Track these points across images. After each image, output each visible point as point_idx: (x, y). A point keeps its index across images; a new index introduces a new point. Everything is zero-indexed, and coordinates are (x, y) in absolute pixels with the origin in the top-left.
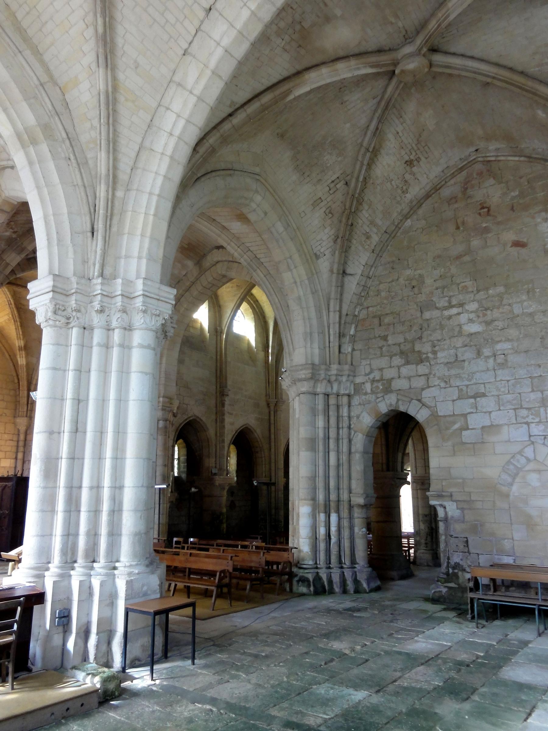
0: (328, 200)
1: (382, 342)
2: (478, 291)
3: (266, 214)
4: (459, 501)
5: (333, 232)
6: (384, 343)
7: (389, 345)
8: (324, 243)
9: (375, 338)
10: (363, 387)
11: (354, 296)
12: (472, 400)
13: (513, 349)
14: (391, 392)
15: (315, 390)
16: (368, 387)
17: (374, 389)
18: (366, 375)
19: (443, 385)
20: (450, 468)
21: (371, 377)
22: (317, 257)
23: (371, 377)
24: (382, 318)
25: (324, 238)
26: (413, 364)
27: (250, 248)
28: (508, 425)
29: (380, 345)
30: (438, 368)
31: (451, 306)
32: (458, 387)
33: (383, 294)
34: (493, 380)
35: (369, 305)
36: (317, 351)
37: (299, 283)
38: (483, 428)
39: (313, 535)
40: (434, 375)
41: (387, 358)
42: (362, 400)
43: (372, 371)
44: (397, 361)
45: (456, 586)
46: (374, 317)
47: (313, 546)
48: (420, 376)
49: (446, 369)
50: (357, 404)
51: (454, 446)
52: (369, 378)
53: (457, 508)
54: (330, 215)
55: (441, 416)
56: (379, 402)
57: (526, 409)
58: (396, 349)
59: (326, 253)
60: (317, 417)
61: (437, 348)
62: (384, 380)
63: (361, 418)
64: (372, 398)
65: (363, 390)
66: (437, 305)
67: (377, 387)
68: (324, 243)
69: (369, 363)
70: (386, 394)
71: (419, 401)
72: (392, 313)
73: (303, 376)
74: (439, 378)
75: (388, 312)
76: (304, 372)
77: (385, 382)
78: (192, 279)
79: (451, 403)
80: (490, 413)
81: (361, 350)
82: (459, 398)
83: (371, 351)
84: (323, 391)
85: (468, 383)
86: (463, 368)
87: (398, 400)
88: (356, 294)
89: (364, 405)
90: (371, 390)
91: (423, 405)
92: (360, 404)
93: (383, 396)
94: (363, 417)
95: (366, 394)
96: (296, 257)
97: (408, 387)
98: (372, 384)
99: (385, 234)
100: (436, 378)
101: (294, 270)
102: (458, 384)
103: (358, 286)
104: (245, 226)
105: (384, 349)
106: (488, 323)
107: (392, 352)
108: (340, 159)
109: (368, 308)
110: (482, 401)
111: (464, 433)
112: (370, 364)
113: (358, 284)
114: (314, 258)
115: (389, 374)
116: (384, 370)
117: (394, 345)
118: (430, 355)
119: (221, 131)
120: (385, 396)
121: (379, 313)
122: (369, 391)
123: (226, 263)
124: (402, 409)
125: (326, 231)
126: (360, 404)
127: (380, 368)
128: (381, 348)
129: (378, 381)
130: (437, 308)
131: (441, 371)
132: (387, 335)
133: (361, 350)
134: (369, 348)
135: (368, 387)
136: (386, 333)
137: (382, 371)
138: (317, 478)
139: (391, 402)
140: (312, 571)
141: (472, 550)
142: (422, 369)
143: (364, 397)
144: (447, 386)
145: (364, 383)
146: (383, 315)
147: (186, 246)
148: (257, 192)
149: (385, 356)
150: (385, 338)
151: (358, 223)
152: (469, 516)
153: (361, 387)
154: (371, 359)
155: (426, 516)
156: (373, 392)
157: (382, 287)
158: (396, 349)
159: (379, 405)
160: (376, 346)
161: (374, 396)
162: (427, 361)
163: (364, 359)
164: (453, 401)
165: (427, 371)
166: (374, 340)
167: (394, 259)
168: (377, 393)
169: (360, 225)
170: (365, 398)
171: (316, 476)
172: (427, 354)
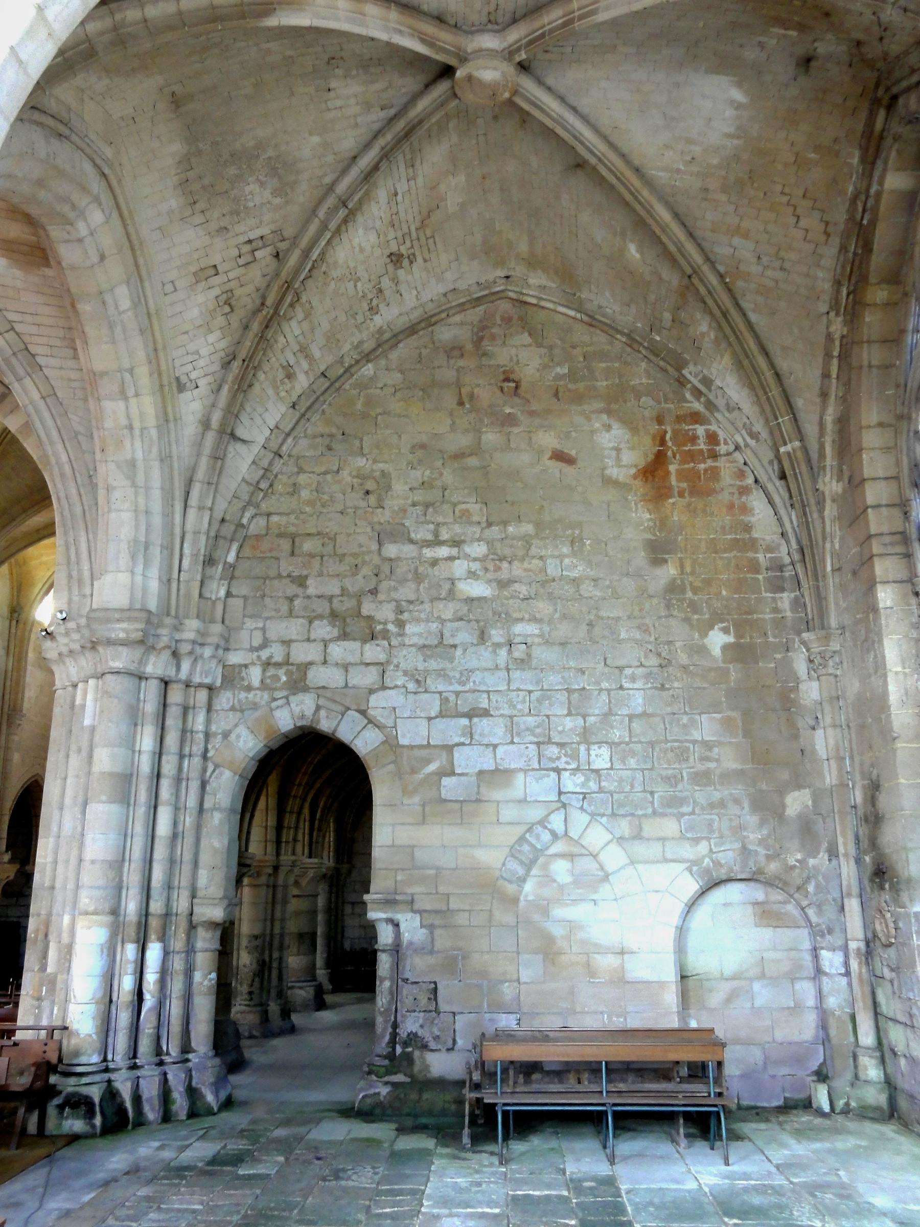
0: (231, 275)
1: (292, 589)
2: (490, 524)
3: (102, 258)
4: (425, 911)
5: (223, 344)
6: (300, 591)
7: (309, 597)
8: (202, 363)
9: (279, 576)
10: (243, 674)
11: (244, 485)
12: (465, 721)
13: (541, 636)
14: (306, 689)
15: (142, 669)
16: (255, 675)
17: (268, 681)
18: (253, 649)
19: (411, 686)
20: (413, 847)
21: (264, 654)
22: (181, 388)
23: (264, 654)
24: (297, 540)
25: (204, 352)
26: (355, 640)
27: (15, 325)
28: (526, 771)
30: (404, 652)
31: (437, 542)
32: (440, 693)
33: (305, 494)
34: (503, 687)
35: (272, 510)
36: (154, 585)
37: (137, 432)
38: (481, 773)
39: (105, 994)
40: (397, 666)
41: (301, 620)
42: (239, 701)
43: (265, 644)
44: (323, 629)
45: (408, 1080)
46: (280, 535)
47: (103, 1020)
48: (368, 664)
49: (421, 658)
50: (227, 707)
51: (424, 806)
52: (259, 657)
53: (422, 926)
54: (227, 309)
55: (403, 746)
56: (278, 707)
57: (557, 744)
58: (322, 607)
59: (201, 383)
60: (139, 728)
61: (406, 616)
62: (292, 664)
63: (233, 736)
64: (263, 697)
65: (243, 679)
66: (413, 535)
67: (276, 678)
68: (202, 363)
69: (260, 625)
70: (294, 694)
71: (363, 713)
72: (319, 534)
73: (122, 635)
74: (405, 673)
75: (314, 531)
76: (124, 625)
77: (294, 668)
79: (425, 723)
80: (495, 746)
81: (245, 598)
82: (441, 715)
83: (267, 600)
84: (159, 672)
85: (459, 688)
86: (451, 660)
87: (318, 708)
88: (247, 483)
89: (242, 711)
91: (370, 722)
92: (233, 709)
93: (287, 697)
94: (238, 736)
95: (249, 688)
96: (143, 372)
97: (341, 683)
98: (264, 671)
99: (322, 379)
100: (400, 673)
101: (133, 402)
102: (441, 688)
103: (253, 467)
104: (17, 273)
105: (297, 602)
106: (503, 584)
107: (314, 611)
108: (278, 201)
109: (269, 515)
110: (482, 724)
111: (446, 781)
112: (264, 630)
113: (254, 462)
114: (174, 384)
115: (302, 653)
116: (293, 645)
117: (319, 597)
118: (391, 627)
119: (118, 17)
120: (292, 698)
121: (292, 529)
122: (256, 682)
124: (325, 725)
125: (212, 338)
126: (233, 709)
127: (287, 638)
128: (291, 600)
129: (278, 665)
130: (411, 541)
131: (408, 659)
132: (306, 577)
133: (245, 598)
134: (263, 596)
135: (255, 675)
136: (305, 573)
137: (289, 646)
138: (127, 864)
139: (302, 711)
140: (97, 1078)
141: (443, 1007)
142: (374, 652)
143: (243, 695)
144: (420, 690)
145: (246, 666)
146: (299, 535)
148: (97, 200)
149: (297, 617)
150: (301, 581)
151: (276, 341)
152: (443, 941)
153: (239, 673)
154: (267, 618)
155: (256, 937)
156: (264, 686)
157: (302, 479)
158: (322, 607)
159: (277, 714)
160: (280, 594)
161: (266, 696)
162: (384, 638)
163: (251, 617)
164: (430, 719)
165: (382, 657)
167: (334, 430)
168: (276, 689)
169: (280, 346)
171: (123, 860)
172: (385, 623)
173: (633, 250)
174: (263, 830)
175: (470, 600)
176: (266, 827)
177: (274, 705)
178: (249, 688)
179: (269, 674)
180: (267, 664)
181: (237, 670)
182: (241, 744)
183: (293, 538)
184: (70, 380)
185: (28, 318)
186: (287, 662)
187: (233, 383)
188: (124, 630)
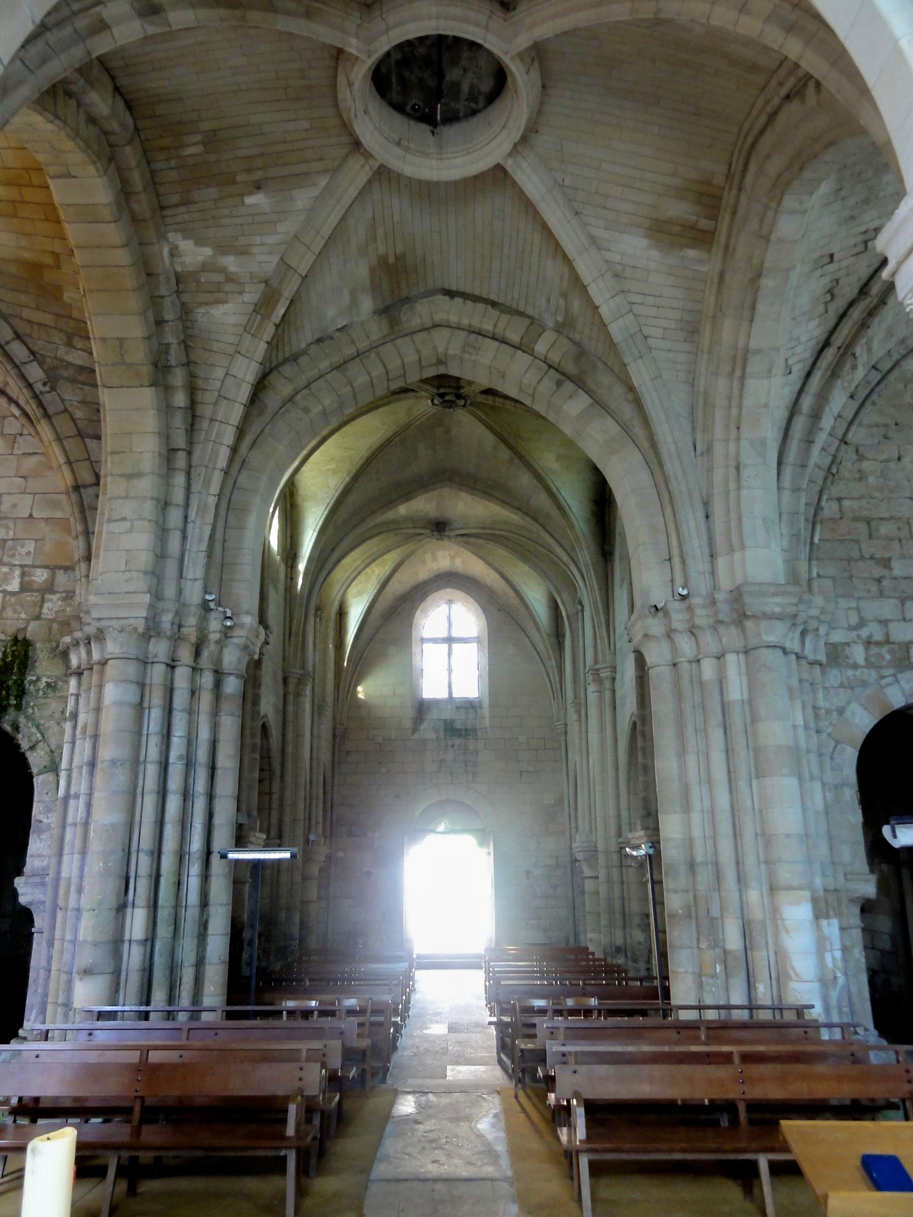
1: (878, 572)
5: (817, 332)
6: (886, 572)
7: (895, 578)
9: (862, 558)
10: (847, 652)
11: (817, 470)
16: (858, 653)
17: (873, 659)
18: (851, 628)
21: (864, 633)
23: (864, 633)
24: (873, 523)
25: (804, 339)
27: (634, 307)
29: (877, 576)
33: (871, 479)
35: (842, 495)
41: (893, 601)
42: (848, 678)
43: (862, 624)
46: (855, 519)
52: (859, 636)
54: (828, 297)
56: (887, 685)
62: (893, 643)
63: (848, 714)
65: (847, 657)
67: (881, 657)
69: (854, 605)
70: (902, 672)
72: (892, 518)
73: (777, 609)
75: (887, 515)
76: (778, 600)
77: (896, 646)
78: (363, 345)
81: (833, 578)
83: (856, 581)
88: (819, 467)
89: (852, 688)
90: (866, 660)
92: (842, 686)
93: (894, 675)
94: (853, 713)
95: (855, 666)
98: (867, 649)
99: (874, 372)
103: (823, 452)
104: (655, 254)
105: (885, 583)
107: (904, 592)
109: (839, 500)
112: (858, 609)
113: (823, 449)
116: (891, 625)
117: (906, 578)
120: (900, 676)
121: (865, 513)
122: (861, 660)
123: (463, 334)
126: (842, 686)
127: (883, 618)
128: (879, 581)
129: (878, 643)
132: (889, 559)
133: (833, 578)
134: (851, 577)
135: (858, 653)
136: (887, 555)
137: (886, 626)
143: (850, 673)
145: (848, 644)
146: (873, 519)
147: (391, 260)
149: (888, 598)
150: (886, 563)
153: (843, 650)
154: (859, 598)
156: (869, 664)
157: (865, 465)
159: (889, 691)
160: (867, 575)
161: (874, 674)
163: (843, 596)
166: (861, 563)
167: (888, 421)
168: (881, 667)
170: (854, 675)
177: (883, 682)
178: (855, 666)
179: (871, 652)
180: (868, 643)
181: (840, 649)
182: (857, 721)
183: (868, 521)
184: (675, 362)
185: (650, 300)
186: (888, 642)
187: (826, 370)
188: (778, 604)
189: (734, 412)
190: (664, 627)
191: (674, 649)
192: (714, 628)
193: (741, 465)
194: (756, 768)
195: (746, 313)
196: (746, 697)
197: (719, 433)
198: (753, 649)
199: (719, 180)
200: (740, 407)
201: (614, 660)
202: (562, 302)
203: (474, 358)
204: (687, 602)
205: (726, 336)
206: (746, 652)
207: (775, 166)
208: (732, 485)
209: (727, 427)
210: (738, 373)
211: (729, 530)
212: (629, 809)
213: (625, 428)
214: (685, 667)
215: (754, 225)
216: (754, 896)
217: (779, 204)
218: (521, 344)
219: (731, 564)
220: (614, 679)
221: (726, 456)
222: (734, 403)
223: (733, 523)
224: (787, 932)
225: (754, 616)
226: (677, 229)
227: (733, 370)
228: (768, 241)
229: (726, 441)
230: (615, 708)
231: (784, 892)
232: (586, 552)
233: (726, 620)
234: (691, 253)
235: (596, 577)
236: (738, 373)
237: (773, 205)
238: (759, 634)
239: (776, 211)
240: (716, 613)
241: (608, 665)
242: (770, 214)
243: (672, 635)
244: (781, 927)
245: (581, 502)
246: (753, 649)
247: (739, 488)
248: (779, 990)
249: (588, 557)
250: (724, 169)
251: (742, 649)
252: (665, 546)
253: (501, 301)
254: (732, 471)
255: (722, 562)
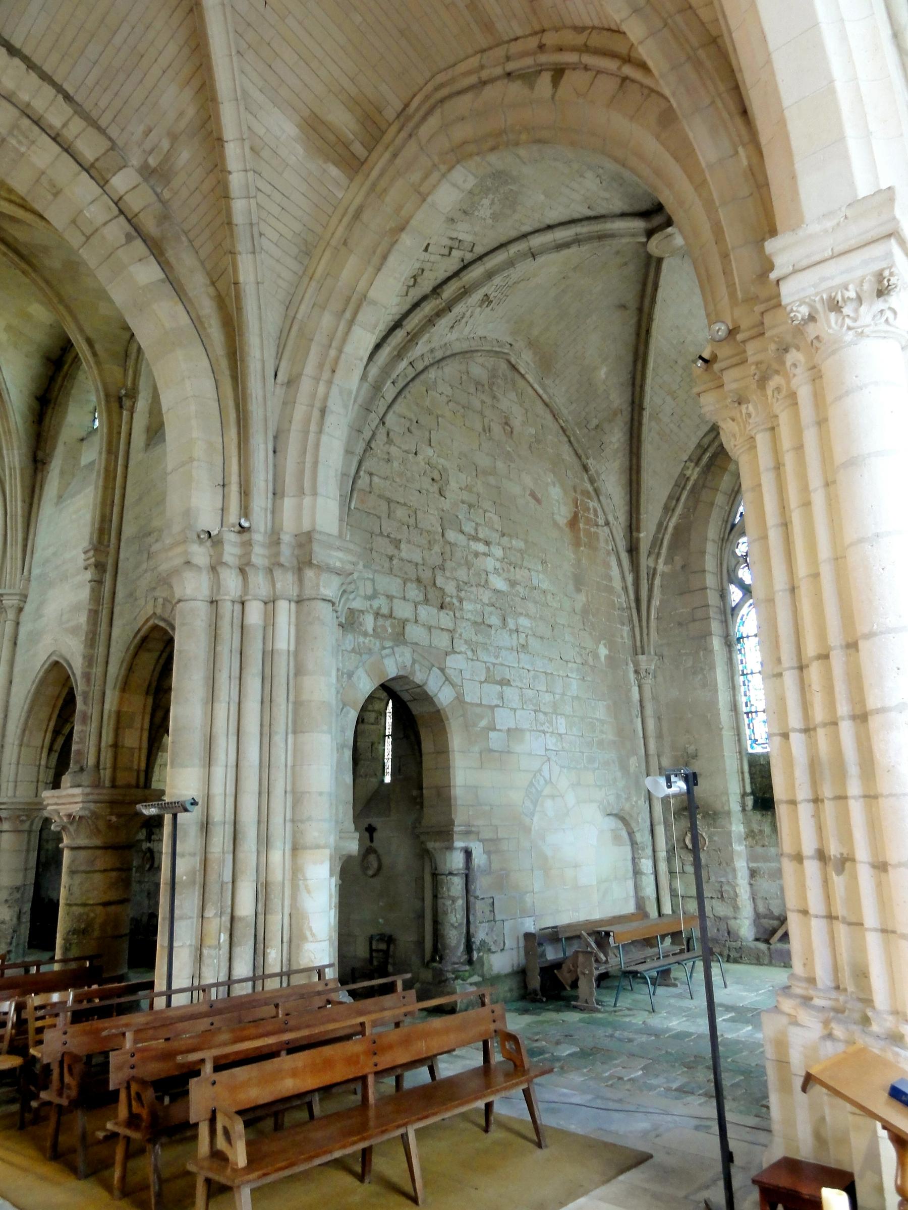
1: (391, 550)
2: (503, 535)
4: (487, 840)
6: (396, 552)
7: (402, 560)
10: (361, 619)
12: (499, 687)
13: (531, 629)
14: (405, 643)
16: (369, 622)
19: (470, 654)
20: (476, 787)
21: (376, 604)
23: (376, 604)
26: (432, 605)
28: (530, 731)
29: (390, 554)
30: (464, 624)
31: (476, 539)
32: (485, 662)
33: (396, 464)
34: (516, 665)
38: (509, 730)
40: (461, 635)
42: (358, 643)
43: (374, 596)
44: (413, 592)
45: (480, 979)
48: (442, 629)
49: (473, 631)
50: (349, 648)
51: (481, 753)
52: (371, 605)
53: (484, 852)
54: (412, 282)
55: (467, 703)
56: (387, 656)
58: (412, 572)
61: (462, 594)
62: (395, 618)
63: (355, 678)
64: (376, 644)
66: (463, 528)
69: (371, 576)
71: (442, 670)
73: (338, 564)
74: (466, 642)
75: (402, 501)
76: (340, 554)
79: (478, 685)
80: (515, 710)
82: (486, 681)
85: (495, 661)
86: (489, 636)
87: (414, 662)
89: (361, 655)
90: (374, 630)
91: (447, 679)
94: (359, 678)
95: (365, 634)
97: (427, 643)
98: (376, 619)
100: (462, 642)
102: (486, 660)
104: (300, 150)
106: (513, 584)
108: (490, 221)
110: (508, 691)
111: (492, 735)
112: (373, 580)
115: (403, 610)
118: (455, 601)
120: (396, 649)
121: (388, 494)
122: (370, 628)
123: (13, 112)
124: (419, 678)
127: (389, 594)
128: (391, 558)
129: (383, 616)
130: (462, 532)
131: (466, 631)
132: (400, 541)
135: (369, 622)
136: (399, 537)
139: (404, 662)
141: (498, 917)
142: (445, 619)
143: (361, 639)
144: (475, 658)
145: (362, 612)
150: (397, 543)
154: (375, 571)
155: (17, 889)
157: (394, 450)
158: (412, 572)
162: (450, 610)
164: (481, 683)
165: (450, 626)
166: (380, 539)
168: (384, 639)
170: (364, 643)
172: (452, 597)
173: (603, 372)
174: (36, 768)
175: (496, 591)
176: (39, 766)
177: (384, 652)
178: (365, 634)
179: (379, 623)
180: (377, 615)
181: (356, 613)
182: (361, 685)
183: (389, 501)
184: (279, 276)
185: (277, 196)
186: (391, 616)
187: (394, 348)
188: (340, 560)
189: (333, 353)
190: (208, 558)
191: (216, 584)
192: (270, 571)
193: (327, 409)
194: (295, 722)
195: (376, 260)
196: (292, 648)
197: (310, 369)
198: (309, 599)
199: (390, 113)
200: (340, 351)
201: (27, 588)
202: (165, 144)
203: (23, 149)
204: (246, 536)
205: (346, 275)
206: (297, 602)
207: (461, 132)
208: (313, 428)
209: (321, 366)
210: (348, 315)
211: (302, 472)
212: (18, 763)
213: (197, 323)
214: (227, 609)
215: (415, 177)
216: (278, 856)
217: (450, 169)
218: (92, 165)
219: (299, 508)
220: (20, 610)
221: (313, 395)
222: (334, 344)
223: (308, 465)
224: (309, 892)
225: (319, 567)
226: (332, 138)
227: (344, 311)
228: (424, 200)
229: (317, 380)
230: (15, 644)
231: (310, 851)
232: (16, 452)
233: (286, 564)
234: (334, 171)
235: (22, 486)
236: (348, 315)
237: (443, 168)
238: (318, 585)
239: (444, 175)
240: (278, 554)
241: (18, 591)
242: (436, 175)
243: (219, 569)
244: (302, 887)
245: (21, 391)
246: (309, 599)
247: (320, 431)
248: (290, 953)
249: (17, 459)
250: (399, 106)
251: (295, 598)
252: (220, 469)
253: (78, 98)
254: (316, 413)
255: (288, 503)
